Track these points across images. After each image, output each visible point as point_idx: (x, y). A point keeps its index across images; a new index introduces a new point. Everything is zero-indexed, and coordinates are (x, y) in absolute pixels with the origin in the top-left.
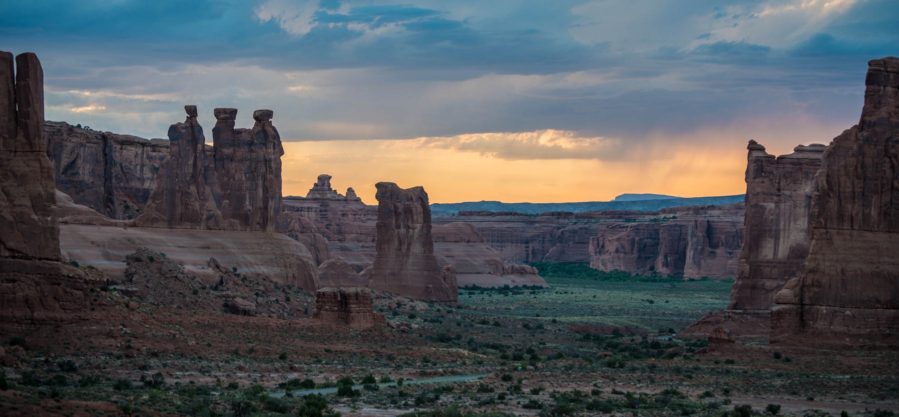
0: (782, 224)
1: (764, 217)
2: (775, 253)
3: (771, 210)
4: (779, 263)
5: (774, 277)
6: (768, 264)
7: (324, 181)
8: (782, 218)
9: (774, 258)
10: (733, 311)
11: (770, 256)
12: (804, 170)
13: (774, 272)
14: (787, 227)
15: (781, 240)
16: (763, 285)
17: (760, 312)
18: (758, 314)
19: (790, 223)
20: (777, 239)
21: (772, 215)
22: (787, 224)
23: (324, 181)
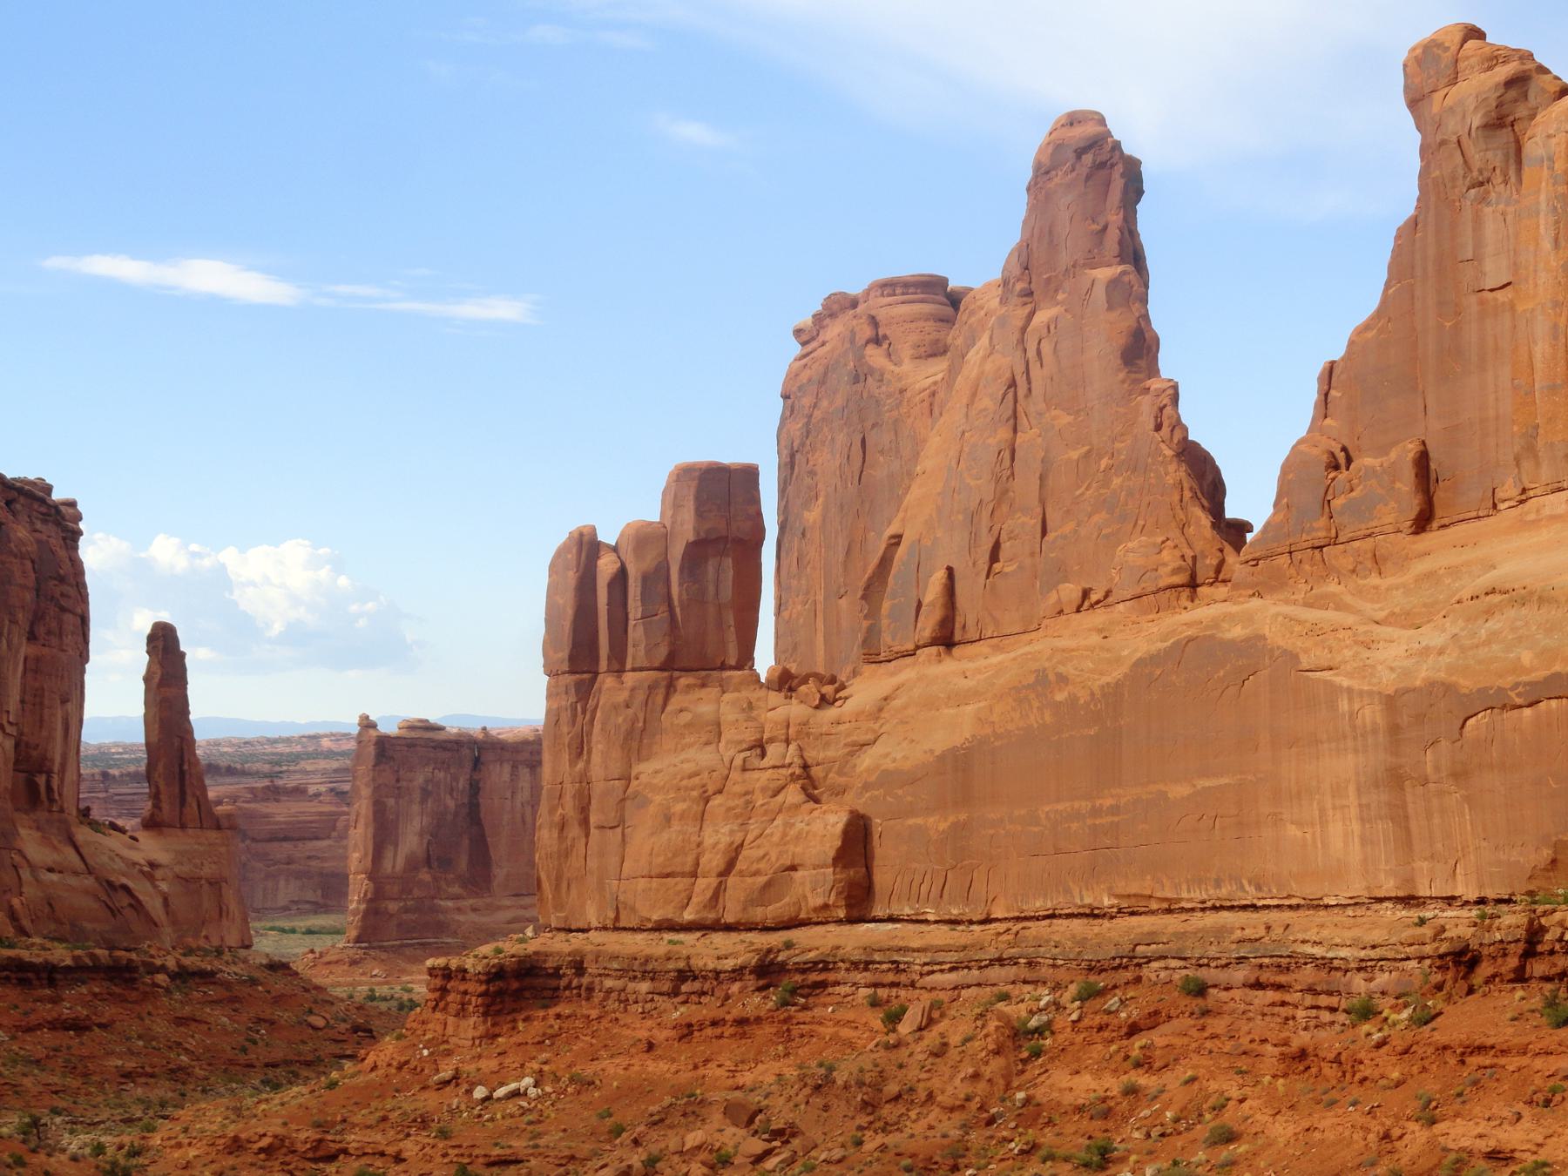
2: (394, 867)
11: (389, 870)
16: (386, 908)
20: (396, 845)
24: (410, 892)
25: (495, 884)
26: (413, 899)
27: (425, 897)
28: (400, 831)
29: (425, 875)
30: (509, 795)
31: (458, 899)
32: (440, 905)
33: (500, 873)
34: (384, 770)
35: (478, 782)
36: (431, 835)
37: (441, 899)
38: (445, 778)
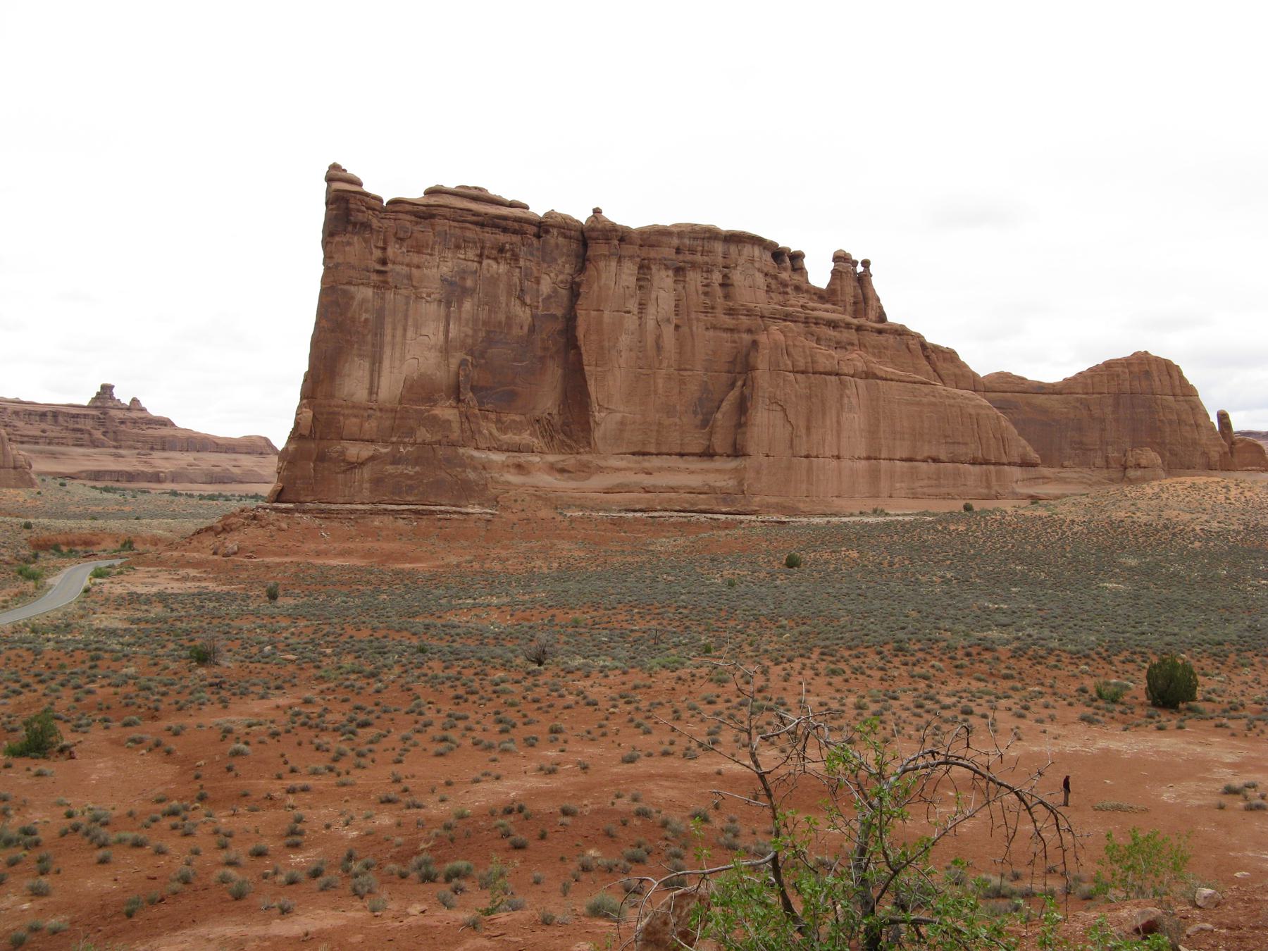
0: (388, 331)
1: (349, 315)
2: (372, 391)
3: (364, 301)
4: (381, 410)
5: (367, 437)
6: (355, 411)
7: (106, 390)
8: (388, 320)
9: (370, 401)
10: (275, 505)
12: (438, 228)
13: (366, 425)
14: (398, 339)
15: (386, 363)
16: (342, 453)
17: (333, 507)
18: (330, 511)
19: (405, 330)
20: (376, 361)
21: (366, 311)
22: (399, 332)
23: (106, 390)
24: (411, 432)
25: (597, 434)
26: (414, 444)
27: (439, 443)
28: (388, 338)
29: (446, 411)
30: (633, 306)
31: (520, 451)
32: (472, 458)
33: (605, 421)
34: (349, 244)
35: (579, 285)
36: (471, 352)
37: (477, 448)
38: (509, 274)
